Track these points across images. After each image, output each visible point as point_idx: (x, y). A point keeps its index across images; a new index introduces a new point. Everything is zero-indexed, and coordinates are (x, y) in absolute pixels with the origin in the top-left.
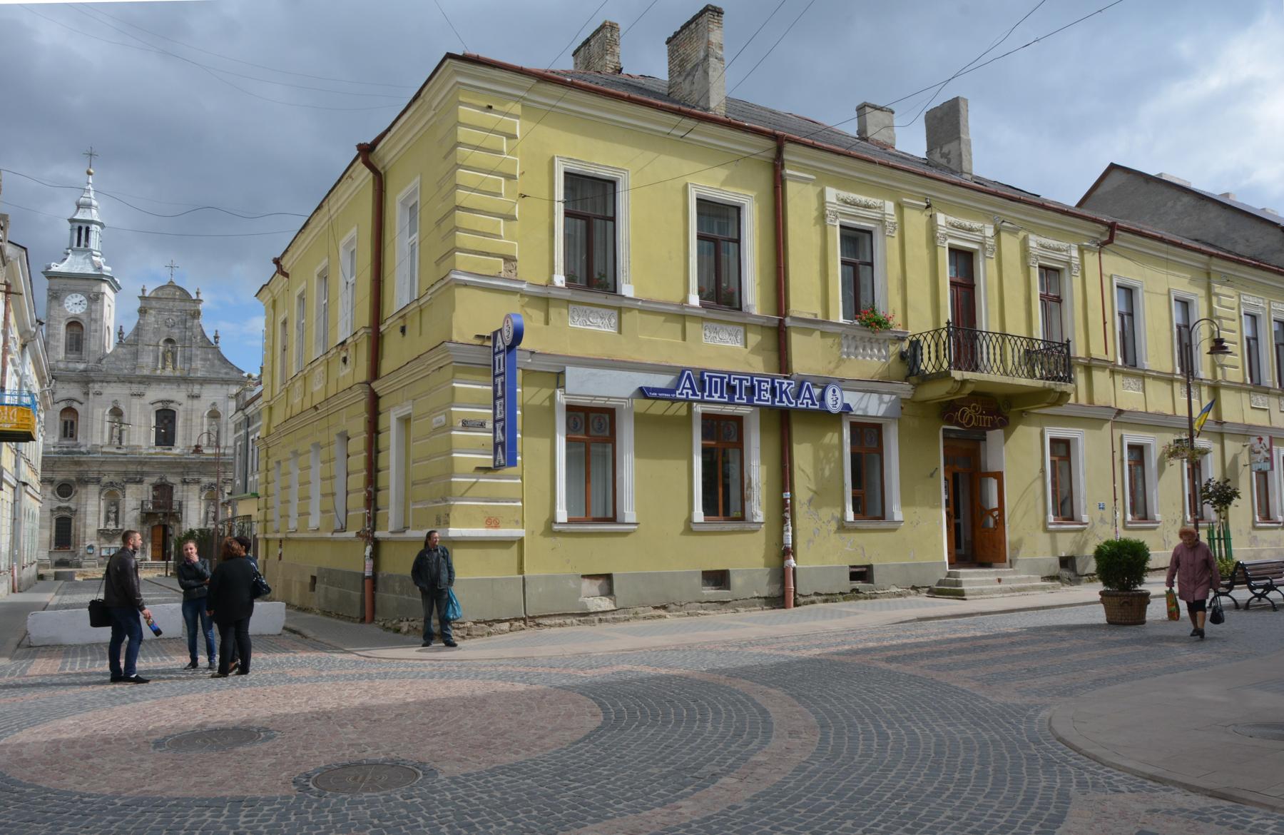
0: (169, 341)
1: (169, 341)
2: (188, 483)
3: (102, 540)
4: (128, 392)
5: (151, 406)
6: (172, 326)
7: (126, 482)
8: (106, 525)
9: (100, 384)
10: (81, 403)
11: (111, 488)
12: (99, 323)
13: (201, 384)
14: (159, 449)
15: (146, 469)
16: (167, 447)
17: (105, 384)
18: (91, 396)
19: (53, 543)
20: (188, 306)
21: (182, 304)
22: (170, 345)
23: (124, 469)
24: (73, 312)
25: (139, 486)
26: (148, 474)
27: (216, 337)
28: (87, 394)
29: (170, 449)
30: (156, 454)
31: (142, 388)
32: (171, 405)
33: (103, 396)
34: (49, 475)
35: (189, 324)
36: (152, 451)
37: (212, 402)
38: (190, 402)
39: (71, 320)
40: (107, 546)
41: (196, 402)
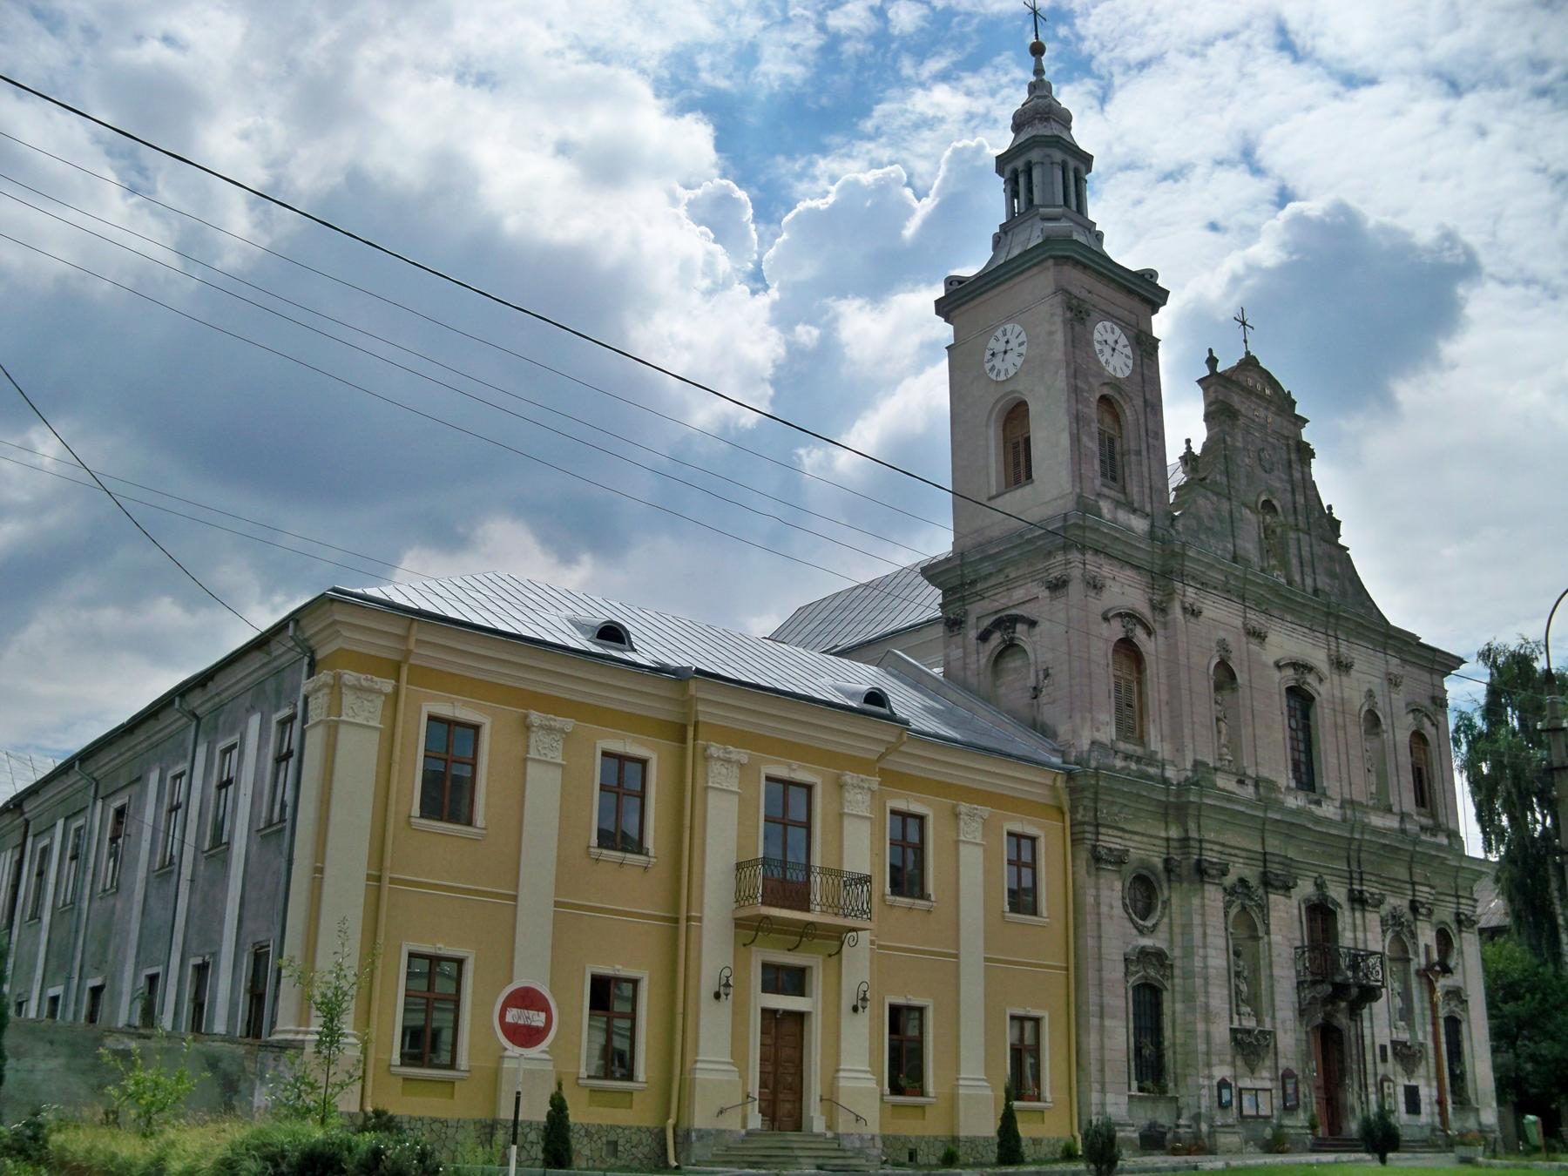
5: (1277, 675)
28: (1160, 609)
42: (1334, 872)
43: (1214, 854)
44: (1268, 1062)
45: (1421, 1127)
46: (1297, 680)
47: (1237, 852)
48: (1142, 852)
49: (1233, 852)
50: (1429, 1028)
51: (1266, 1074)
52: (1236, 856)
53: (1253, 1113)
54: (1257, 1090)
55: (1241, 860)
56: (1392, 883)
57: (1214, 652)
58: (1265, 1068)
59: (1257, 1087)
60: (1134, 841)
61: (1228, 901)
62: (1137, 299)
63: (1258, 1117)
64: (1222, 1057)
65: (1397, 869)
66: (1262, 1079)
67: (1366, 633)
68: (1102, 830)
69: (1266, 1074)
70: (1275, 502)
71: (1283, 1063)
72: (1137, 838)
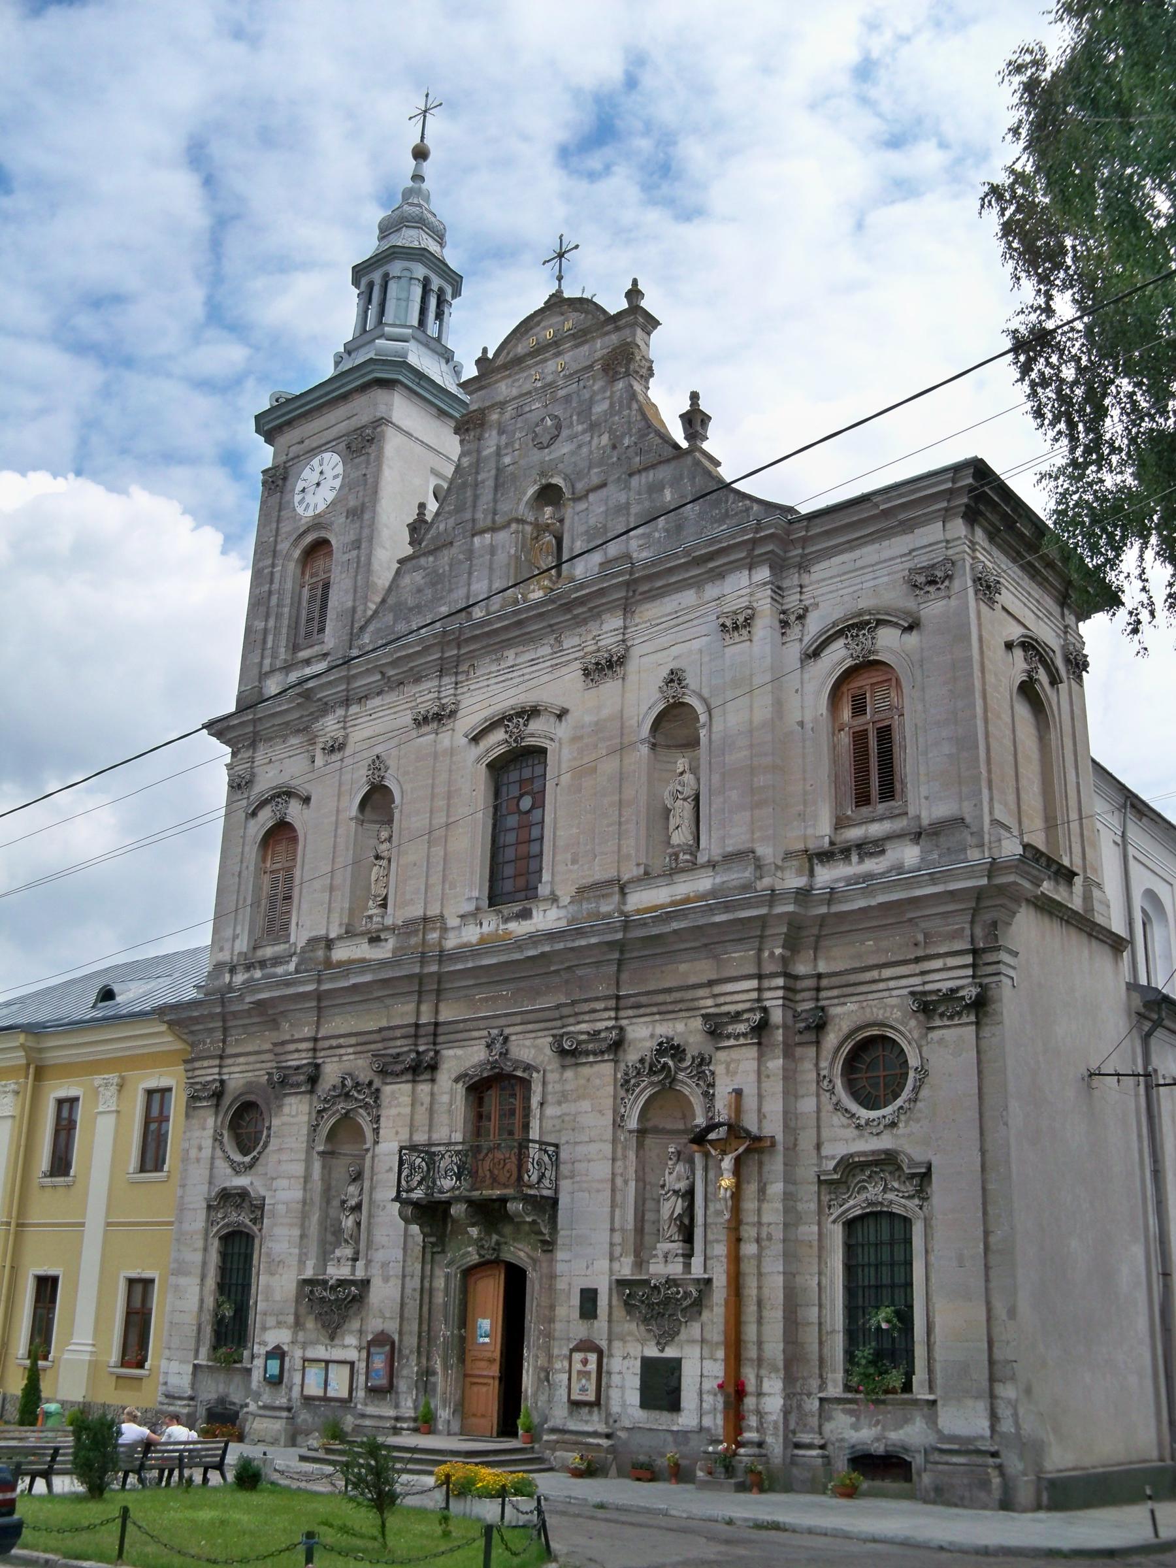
0: (549, 495)
1: (549, 495)
2: (573, 1053)
3: (310, 1324)
7: (383, 1072)
8: (324, 1257)
9: (340, 712)
11: (342, 1106)
12: (367, 516)
14: (491, 924)
15: (447, 1014)
16: (516, 907)
17: (354, 709)
18: (319, 761)
19: (208, 1331)
20: (601, 346)
22: (548, 510)
23: (384, 1024)
24: (310, 513)
25: (424, 1088)
26: (459, 1032)
27: (695, 420)
29: (525, 914)
30: (482, 940)
32: (535, 726)
33: (349, 751)
34: (208, 1073)
35: (600, 408)
36: (471, 934)
37: (664, 673)
39: (309, 539)
40: (320, 1352)
41: (610, 687)
42: (540, 1015)
43: (304, 1055)
44: (355, 1325)
45: (682, 1436)
47: (341, 1041)
48: (250, 1074)
49: (334, 1042)
50: (720, 1250)
51: (351, 1340)
52: (340, 1047)
53: (321, 1393)
54: (327, 1362)
55: (351, 1050)
56: (660, 998)
57: (365, 779)
58: (351, 1332)
59: (327, 1357)
60: (239, 1065)
61: (319, 1112)
62: (356, 396)
63: (325, 1399)
64: (281, 1318)
65: (683, 967)
66: (345, 1347)
67: (659, 584)
68: (197, 1064)
69: (351, 1340)
70: (554, 481)
71: (375, 1325)
72: (241, 1060)
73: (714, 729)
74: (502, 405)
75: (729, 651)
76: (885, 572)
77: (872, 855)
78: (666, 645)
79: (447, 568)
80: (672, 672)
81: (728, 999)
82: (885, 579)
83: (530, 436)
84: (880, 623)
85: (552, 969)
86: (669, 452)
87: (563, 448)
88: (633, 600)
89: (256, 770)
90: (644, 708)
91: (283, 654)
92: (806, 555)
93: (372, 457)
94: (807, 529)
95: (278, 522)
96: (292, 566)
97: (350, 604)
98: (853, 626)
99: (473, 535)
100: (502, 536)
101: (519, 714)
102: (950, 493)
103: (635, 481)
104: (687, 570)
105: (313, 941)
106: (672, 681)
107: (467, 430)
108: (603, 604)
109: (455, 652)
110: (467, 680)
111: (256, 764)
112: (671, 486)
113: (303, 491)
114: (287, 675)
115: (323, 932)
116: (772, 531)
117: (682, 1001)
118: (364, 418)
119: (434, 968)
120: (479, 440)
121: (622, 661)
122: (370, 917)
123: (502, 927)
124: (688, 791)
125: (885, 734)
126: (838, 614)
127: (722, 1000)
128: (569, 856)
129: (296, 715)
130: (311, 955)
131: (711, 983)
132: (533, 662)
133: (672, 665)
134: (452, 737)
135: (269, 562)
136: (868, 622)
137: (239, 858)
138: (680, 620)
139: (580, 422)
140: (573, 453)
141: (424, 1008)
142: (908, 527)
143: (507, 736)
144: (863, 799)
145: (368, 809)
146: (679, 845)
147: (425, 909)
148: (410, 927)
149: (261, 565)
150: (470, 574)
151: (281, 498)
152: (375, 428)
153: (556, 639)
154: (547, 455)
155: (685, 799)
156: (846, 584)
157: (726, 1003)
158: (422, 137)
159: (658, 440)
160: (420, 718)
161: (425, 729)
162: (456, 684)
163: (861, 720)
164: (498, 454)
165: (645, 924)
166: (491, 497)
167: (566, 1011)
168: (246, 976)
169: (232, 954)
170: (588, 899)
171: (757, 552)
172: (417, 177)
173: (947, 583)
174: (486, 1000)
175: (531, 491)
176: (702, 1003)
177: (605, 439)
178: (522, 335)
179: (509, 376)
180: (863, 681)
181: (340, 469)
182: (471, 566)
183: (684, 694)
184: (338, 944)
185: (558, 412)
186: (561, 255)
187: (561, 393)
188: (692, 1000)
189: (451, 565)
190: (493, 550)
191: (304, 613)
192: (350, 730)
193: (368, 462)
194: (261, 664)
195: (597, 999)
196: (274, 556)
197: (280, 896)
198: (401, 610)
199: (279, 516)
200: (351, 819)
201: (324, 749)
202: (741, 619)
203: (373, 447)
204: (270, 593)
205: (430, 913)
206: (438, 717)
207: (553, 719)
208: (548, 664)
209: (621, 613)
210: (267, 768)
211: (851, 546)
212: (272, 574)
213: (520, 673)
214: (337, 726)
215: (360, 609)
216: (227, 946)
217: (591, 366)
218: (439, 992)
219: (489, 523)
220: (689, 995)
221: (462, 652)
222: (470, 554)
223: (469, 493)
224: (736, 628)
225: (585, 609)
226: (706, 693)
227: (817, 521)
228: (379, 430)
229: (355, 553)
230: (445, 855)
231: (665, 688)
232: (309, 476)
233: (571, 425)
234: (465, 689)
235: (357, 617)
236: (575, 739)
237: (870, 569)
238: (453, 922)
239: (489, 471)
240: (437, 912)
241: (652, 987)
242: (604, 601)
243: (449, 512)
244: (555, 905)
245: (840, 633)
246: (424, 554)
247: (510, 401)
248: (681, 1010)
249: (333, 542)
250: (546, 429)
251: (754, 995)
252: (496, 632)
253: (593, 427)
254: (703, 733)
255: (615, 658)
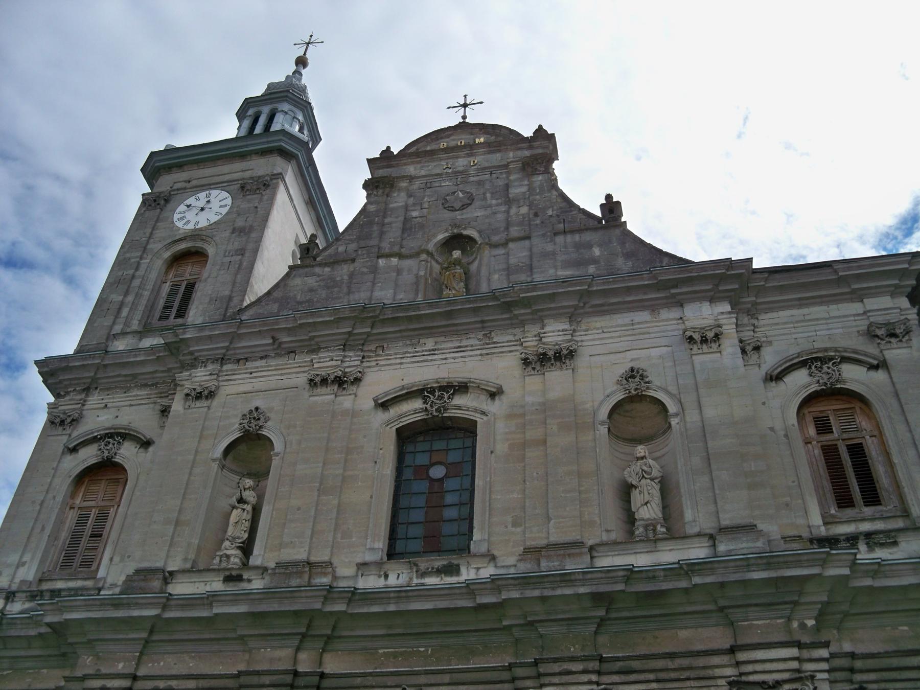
0: (458, 241)
1: (458, 241)
4: (302, 379)
6: (464, 207)
10: (146, 444)
13: (573, 317)
16: (439, 562)
18: (177, 405)
21: (498, 156)
22: (457, 254)
24: (191, 226)
28: (165, 411)
31: (351, 362)
32: (458, 400)
33: (216, 402)
35: (517, 190)
38: (534, 382)
39: (183, 246)
46: (426, 410)
56: (660, 664)
57: (237, 426)
65: (683, 634)
73: (688, 419)
74: (411, 178)
75: (697, 359)
76: (840, 325)
77: (882, 545)
78: (621, 350)
79: (346, 277)
80: (632, 370)
81: (759, 667)
82: (841, 331)
83: (440, 202)
84: (845, 360)
85: (505, 623)
86: (592, 223)
87: (476, 212)
88: (582, 311)
89: (84, 412)
90: (600, 397)
91: (135, 325)
92: (756, 304)
93: (265, 197)
94: (766, 280)
95: (153, 229)
96: (159, 264)
97: (227, 293)
98: (816, 359)
99: (378, 257)
100: (407, 263)
101: (442, 388)
102: (903, 274)
103: (560, 239)
104: (645, 293)
105: (144, 573)
106: (633, 377)
107: (377, 187)
108: (550, 309)
109: (369, 330)
110: (377, 356)
111: (86, 407)
112: (600, 246)
113: (188, 206)
114: (140, 339)
115: (159, 564)
116: (744, 271)
117: (690, 668)
118: (260, 172)
119: (340, 607)
120: (387, 196)
121: (571, 354)
122: (228, 557)
123: (416, 581)
124: (655, 473)
125: (857, 451)
126: (794, 351)
127: (749, 668)
128: (510, 520)
129: (149, 369)
130: (143, 584)
131: (732, 650)
132: (459, 349)
133: (636, 365)
134: (354, 400)
135: (139, 254)
136: (831, 359)
137: (46, 487)
138: (637, 331)
139: (492, 198)
140: (487, 217)
141: (303, 656)
142: (858, 296)
143: (428, 406)
144: (844, 501)
145: (230, 457)
146: (649, 519)
147: (309, 554)
148: (286, 568)
149: (128, 255)
150: (374, 284)
151: (160, 213)
152: (271, 179)
153: (485, 335)
154: (458, 215)
155: (652, 479)
156: (800, 330)
157: (756, 672)
158: (305, 54)
159: (581, 216)
160: (318, 379)
161: (320, 390)
162: (363, 357)
163: (828, 437)
164: (406, 208)
165: (654, 577)
166: (399, 233)
167: (519, 672)
168: (27, 605)
169: (11, 581)
170: (548, 557)
171: (721, 288)
172: (297, 73)
173: (907, 338)
174: (395, 656)
175: (441, 237)
176: (718, 672)
177: (524, 210)
178: (432, 140)
179: (420, 162)
180: (827, 408)
181: (229, 201)
182: (374, 278)
183: (648, 388)
184: (180, 578)
185: (472, 189)
186: (465, 105)
187: (472, 179)
188: (704, 668)
189: (351, 275)
190: (399, 271)
191: (161, 303)
192: (221, 384)
193: (261, 200)
194: (111, 328)
195: (573, 659)
196: (144, 252)
197: (88, 530)
198: (288, 303)
199: (155, 225)
200: (214, 460)
201: (187, 395)
202: (710, 335)
203: (268, 191)
204: (133, 277)
205: (313, 559)
206: (340, 382)
207: (484, 397)
208: (478, 352)
209: (568, 320)
210: (100, 412)
211: (802, 303)
212: (139, 263)
213: (443, 356)
214: (208, 378)
215: (236, 301)
216: (10, 571)
217: (506, 166)
218: (329, 639)
219: (396, 249)
220: (701, 661)
221: (375, 331)
222: (374, 270)
223: (375, 228)
224: (704, 340)
225: (529, 311)
226: (673, 389)
227: (777, 276)
228: (274, 181)
229: (240, 257)
230: (339, 505)
231: (624, 382)
232: (197, 200)
233: (485, 199)
234: (374, 363)
235: (232, 304)
236: (510, 416)
237: (824, 322)
238: (345, 570)
239: (397, 217)
240: (326, 558)
241: (642, 650)
242: (552, 305)
243: (351, 240)
244: (492, 564)
245: (803, 364)
246: (320, 265)
247: (419, 177)
248: (688, 679)
249: (211, 250)
250: (457, 198)
251: (795, 665)
252: (419, 318)
253: (509, 202)
254: (674, 422)
255: (565, 352)
